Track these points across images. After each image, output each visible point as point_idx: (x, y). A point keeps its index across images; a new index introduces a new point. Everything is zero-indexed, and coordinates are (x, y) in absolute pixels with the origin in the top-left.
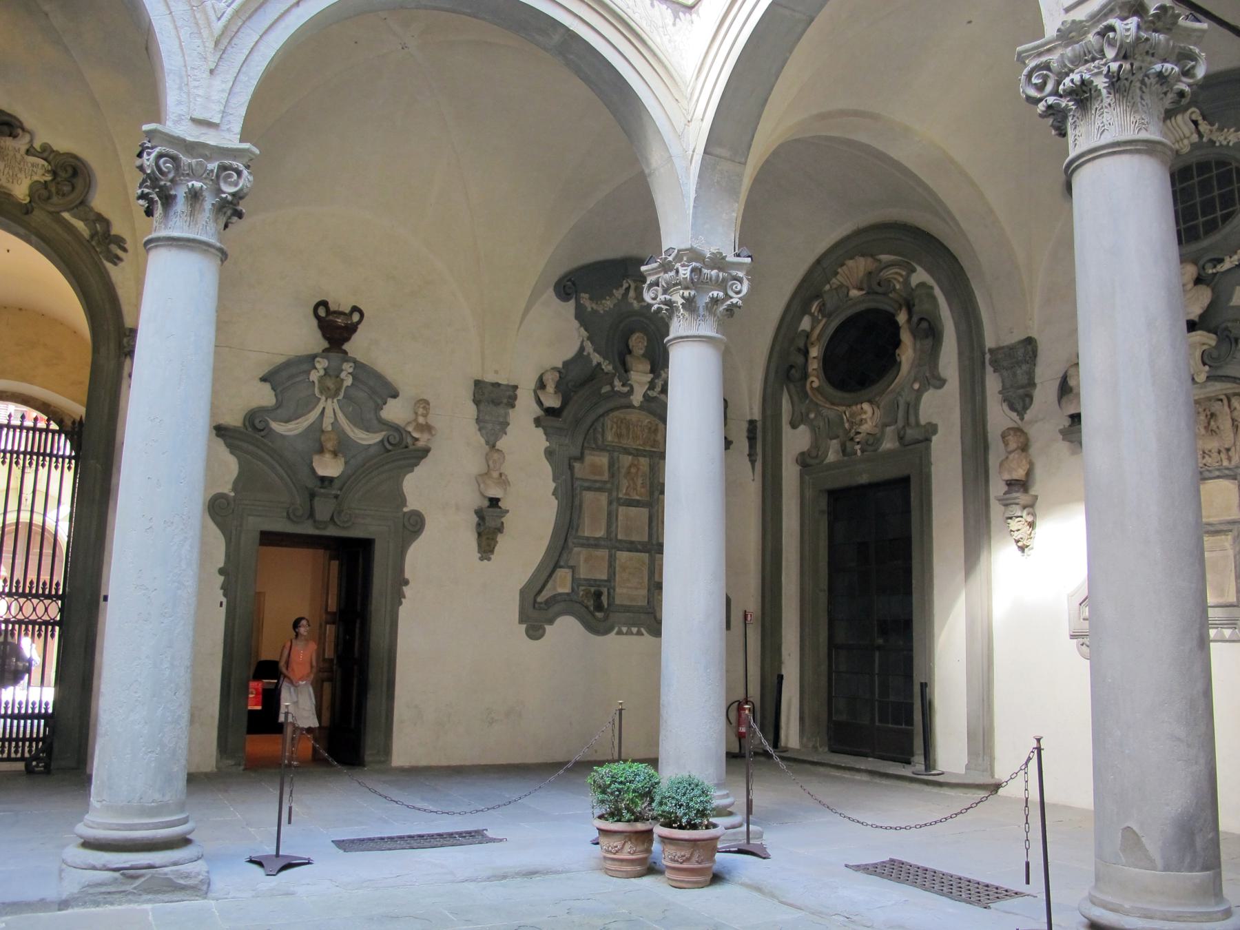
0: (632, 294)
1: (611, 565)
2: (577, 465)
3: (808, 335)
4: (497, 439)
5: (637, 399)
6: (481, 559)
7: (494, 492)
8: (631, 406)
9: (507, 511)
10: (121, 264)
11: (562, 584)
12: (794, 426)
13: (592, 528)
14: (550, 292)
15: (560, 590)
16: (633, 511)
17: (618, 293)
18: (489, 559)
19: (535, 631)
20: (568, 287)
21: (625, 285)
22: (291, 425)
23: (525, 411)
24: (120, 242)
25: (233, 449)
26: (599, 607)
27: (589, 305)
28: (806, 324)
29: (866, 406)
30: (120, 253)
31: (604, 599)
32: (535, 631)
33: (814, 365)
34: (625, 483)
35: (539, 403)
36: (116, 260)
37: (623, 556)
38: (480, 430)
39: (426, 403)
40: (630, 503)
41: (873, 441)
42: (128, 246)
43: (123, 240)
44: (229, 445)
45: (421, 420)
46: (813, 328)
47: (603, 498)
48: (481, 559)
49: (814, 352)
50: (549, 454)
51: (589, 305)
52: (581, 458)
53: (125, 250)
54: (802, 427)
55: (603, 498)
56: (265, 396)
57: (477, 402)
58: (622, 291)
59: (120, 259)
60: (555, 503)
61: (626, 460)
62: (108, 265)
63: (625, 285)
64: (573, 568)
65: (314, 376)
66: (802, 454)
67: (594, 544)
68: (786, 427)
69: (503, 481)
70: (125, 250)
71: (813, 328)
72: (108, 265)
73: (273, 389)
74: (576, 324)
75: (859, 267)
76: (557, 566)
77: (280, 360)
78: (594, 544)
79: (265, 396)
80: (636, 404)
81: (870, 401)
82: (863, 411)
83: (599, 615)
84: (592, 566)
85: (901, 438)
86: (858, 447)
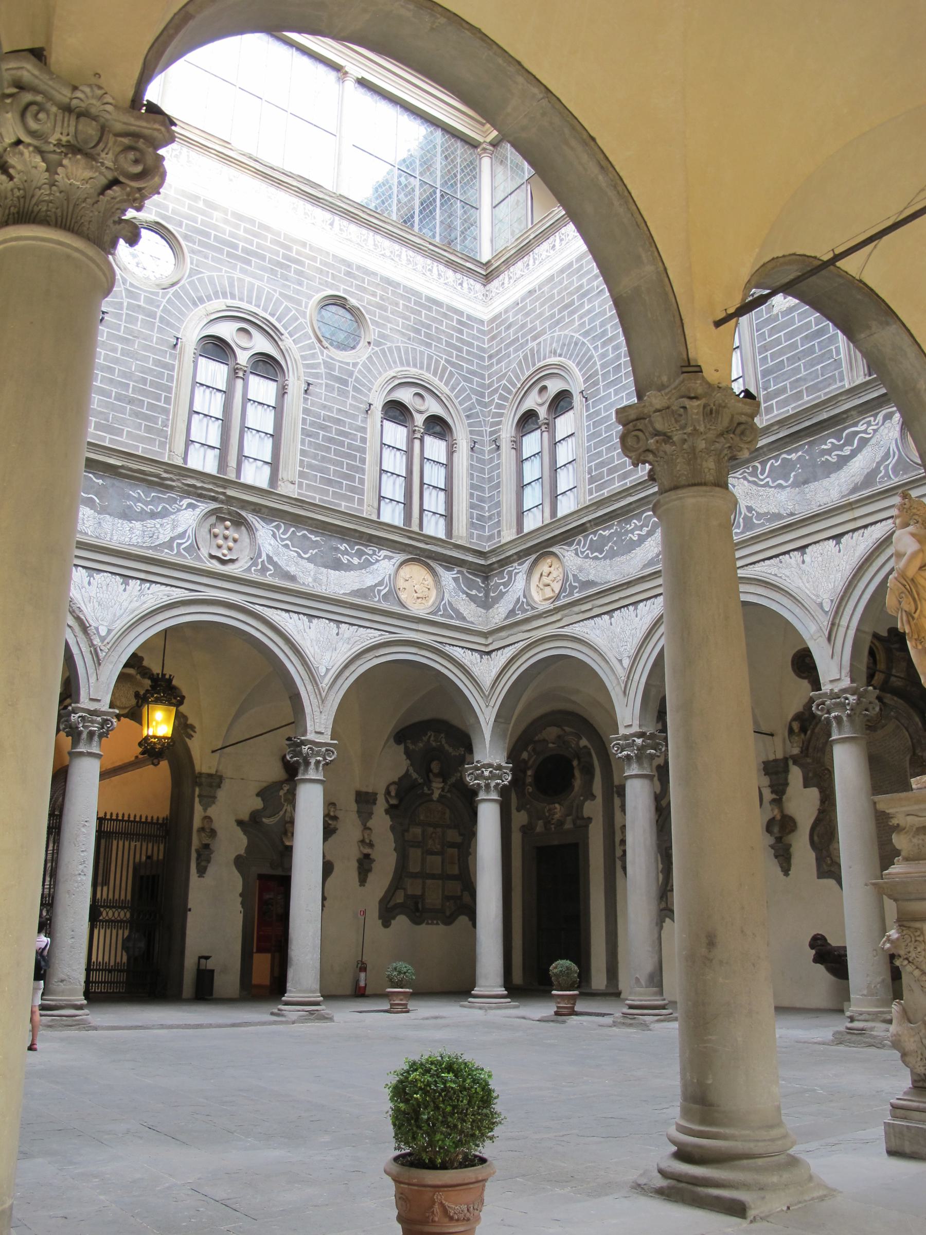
0: (432, 738)
1: (423, 888)
2: (406, 834)
3: (525, 762)
4: (368, 821)
5: (436, 796)
6: (360, 886)
7: (367, 850)
8: (432, 800)
9: (374, 861)
10: (193, 739)
11: (399, 898)
12: (518, 810)
13: (414, 867)
14: (392, 740)
15: (398, 901)
16: (433, 858)
17: (425, 739)
18: (364, 886)
19: (386, 924)
20: (402, 736)
21: (429, 734)
22: (271, 820)
23: (381, 806)
24: (192, 728)
25: (245, 832)
26: (417, 910)
27: (411, 747)
28: (525, 755)
29: (557, 806)
30: (193, 733)
31: (420, 906)
32: (386, 924)
33: (529, 780)
34: (430, 842)
35: (387, 801)
36: (190, 737)
37: (429, 882)
38: (359, 817)
39: (333, 804)
40: (432, 853)
41: (561, 823)
42: (196, 730)
43: (195, 727)
44: (243, 830)
45: (332, 814)
46: (529, 759)
47: (419, 852)
48: (360, 886)
49: (529, 773)
50: (392, 828)
51: (411, 747)
52: (407, 830)
53: (195, 732)
54: (523, 812)
55: (419, 852)
56: (258, 804)
57: (357, 801)
58: (427, 737)
59: (192, 736)
60: (395, 854)
61: (431, 830)
62: (187, 740)
63: (429, 734)
64: (405, 889)
65: (282, 793)
66: (523, 826)
67: (414, 876)
68: (514, 811)
69: (371, 845)
70: (195, 732)
71: (529, 759)
72: (187, 740)
73: (263, 800)
74: (404, 757)
75: (552, 732)
76: (397, 888)
77: (265, 785)
78: (414, 876)
79: (258, 804)
80: (435, 799)
81: (559, 803)
82: (556, 808)
83: (418, 914)
84: (413, 888)
85: (574, 824)
86: (553, 826)
